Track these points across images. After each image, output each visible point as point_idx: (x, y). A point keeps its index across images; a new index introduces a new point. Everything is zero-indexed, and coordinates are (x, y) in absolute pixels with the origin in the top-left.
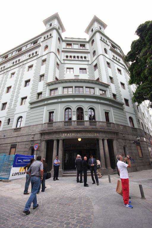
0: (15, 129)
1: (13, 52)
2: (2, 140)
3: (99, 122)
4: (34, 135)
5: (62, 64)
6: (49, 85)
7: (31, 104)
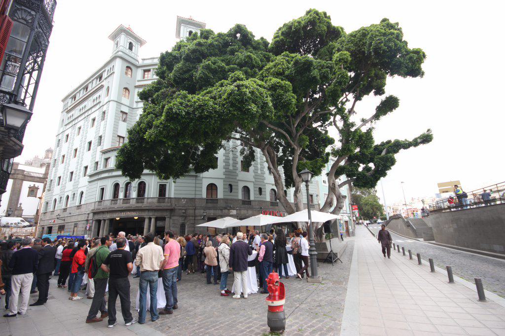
0: (78, 206)
1: (80, 91)
2: (69, 218)
3: (148, 198)
4: (88, 214)
5: (134, 110)
6: (104, 152)
7: (91, 176)
